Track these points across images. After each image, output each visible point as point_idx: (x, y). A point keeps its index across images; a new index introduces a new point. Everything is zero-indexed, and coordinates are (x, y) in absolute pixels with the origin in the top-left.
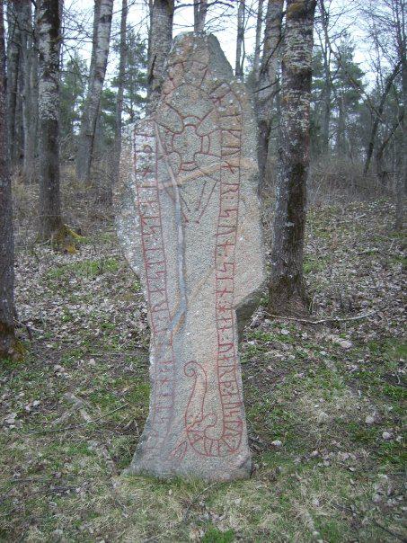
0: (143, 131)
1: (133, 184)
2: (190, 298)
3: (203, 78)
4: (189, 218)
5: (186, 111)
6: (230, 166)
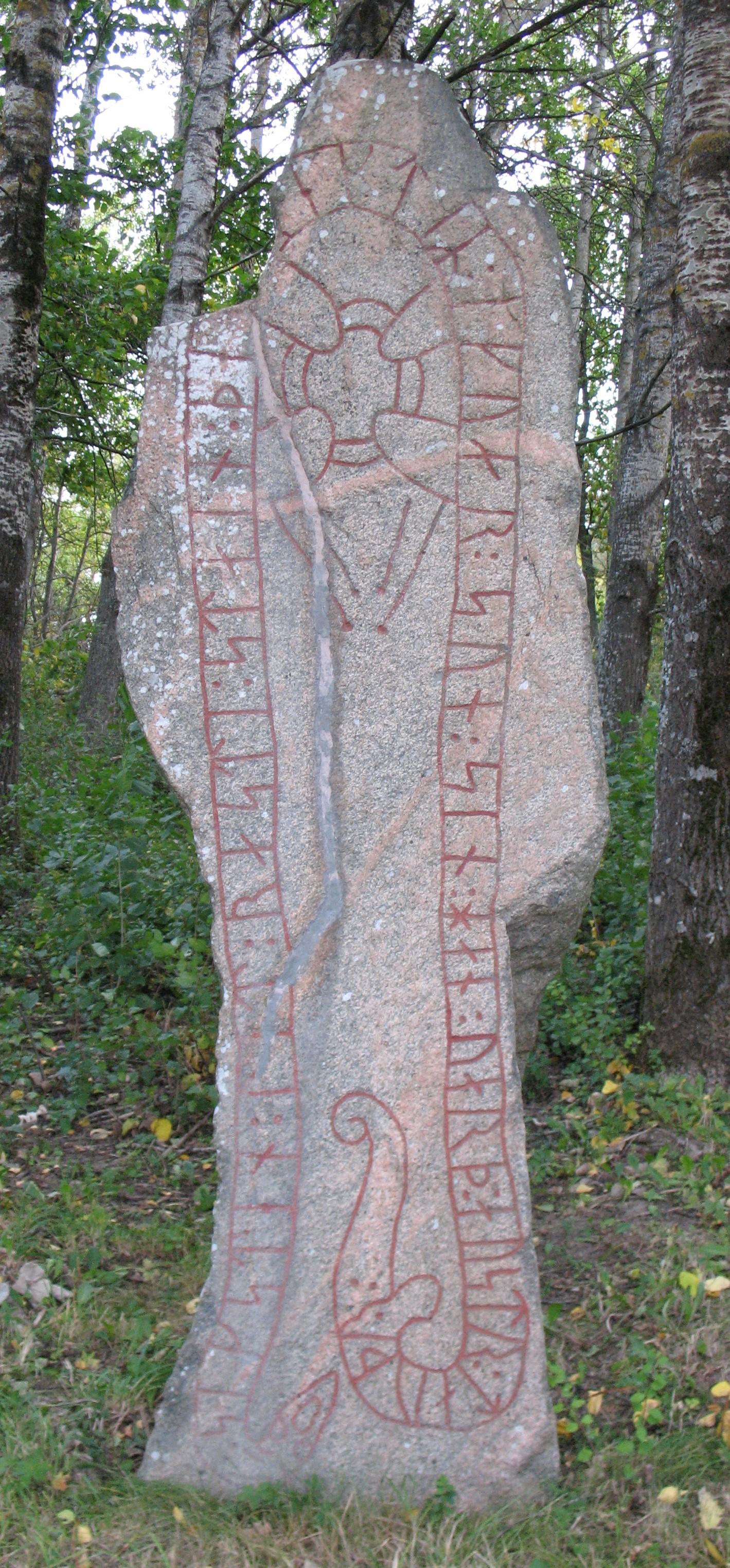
0: (215, 341)
1: (177, 501)
2: (354, 875)
3: (404, 191)
4: (352, 613)
5: (347, 282)
6: (487, 455)
